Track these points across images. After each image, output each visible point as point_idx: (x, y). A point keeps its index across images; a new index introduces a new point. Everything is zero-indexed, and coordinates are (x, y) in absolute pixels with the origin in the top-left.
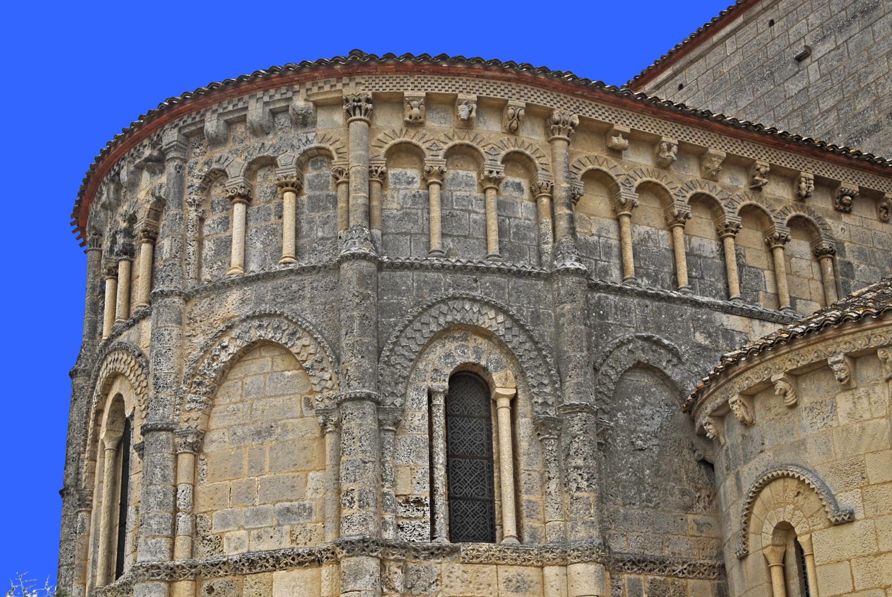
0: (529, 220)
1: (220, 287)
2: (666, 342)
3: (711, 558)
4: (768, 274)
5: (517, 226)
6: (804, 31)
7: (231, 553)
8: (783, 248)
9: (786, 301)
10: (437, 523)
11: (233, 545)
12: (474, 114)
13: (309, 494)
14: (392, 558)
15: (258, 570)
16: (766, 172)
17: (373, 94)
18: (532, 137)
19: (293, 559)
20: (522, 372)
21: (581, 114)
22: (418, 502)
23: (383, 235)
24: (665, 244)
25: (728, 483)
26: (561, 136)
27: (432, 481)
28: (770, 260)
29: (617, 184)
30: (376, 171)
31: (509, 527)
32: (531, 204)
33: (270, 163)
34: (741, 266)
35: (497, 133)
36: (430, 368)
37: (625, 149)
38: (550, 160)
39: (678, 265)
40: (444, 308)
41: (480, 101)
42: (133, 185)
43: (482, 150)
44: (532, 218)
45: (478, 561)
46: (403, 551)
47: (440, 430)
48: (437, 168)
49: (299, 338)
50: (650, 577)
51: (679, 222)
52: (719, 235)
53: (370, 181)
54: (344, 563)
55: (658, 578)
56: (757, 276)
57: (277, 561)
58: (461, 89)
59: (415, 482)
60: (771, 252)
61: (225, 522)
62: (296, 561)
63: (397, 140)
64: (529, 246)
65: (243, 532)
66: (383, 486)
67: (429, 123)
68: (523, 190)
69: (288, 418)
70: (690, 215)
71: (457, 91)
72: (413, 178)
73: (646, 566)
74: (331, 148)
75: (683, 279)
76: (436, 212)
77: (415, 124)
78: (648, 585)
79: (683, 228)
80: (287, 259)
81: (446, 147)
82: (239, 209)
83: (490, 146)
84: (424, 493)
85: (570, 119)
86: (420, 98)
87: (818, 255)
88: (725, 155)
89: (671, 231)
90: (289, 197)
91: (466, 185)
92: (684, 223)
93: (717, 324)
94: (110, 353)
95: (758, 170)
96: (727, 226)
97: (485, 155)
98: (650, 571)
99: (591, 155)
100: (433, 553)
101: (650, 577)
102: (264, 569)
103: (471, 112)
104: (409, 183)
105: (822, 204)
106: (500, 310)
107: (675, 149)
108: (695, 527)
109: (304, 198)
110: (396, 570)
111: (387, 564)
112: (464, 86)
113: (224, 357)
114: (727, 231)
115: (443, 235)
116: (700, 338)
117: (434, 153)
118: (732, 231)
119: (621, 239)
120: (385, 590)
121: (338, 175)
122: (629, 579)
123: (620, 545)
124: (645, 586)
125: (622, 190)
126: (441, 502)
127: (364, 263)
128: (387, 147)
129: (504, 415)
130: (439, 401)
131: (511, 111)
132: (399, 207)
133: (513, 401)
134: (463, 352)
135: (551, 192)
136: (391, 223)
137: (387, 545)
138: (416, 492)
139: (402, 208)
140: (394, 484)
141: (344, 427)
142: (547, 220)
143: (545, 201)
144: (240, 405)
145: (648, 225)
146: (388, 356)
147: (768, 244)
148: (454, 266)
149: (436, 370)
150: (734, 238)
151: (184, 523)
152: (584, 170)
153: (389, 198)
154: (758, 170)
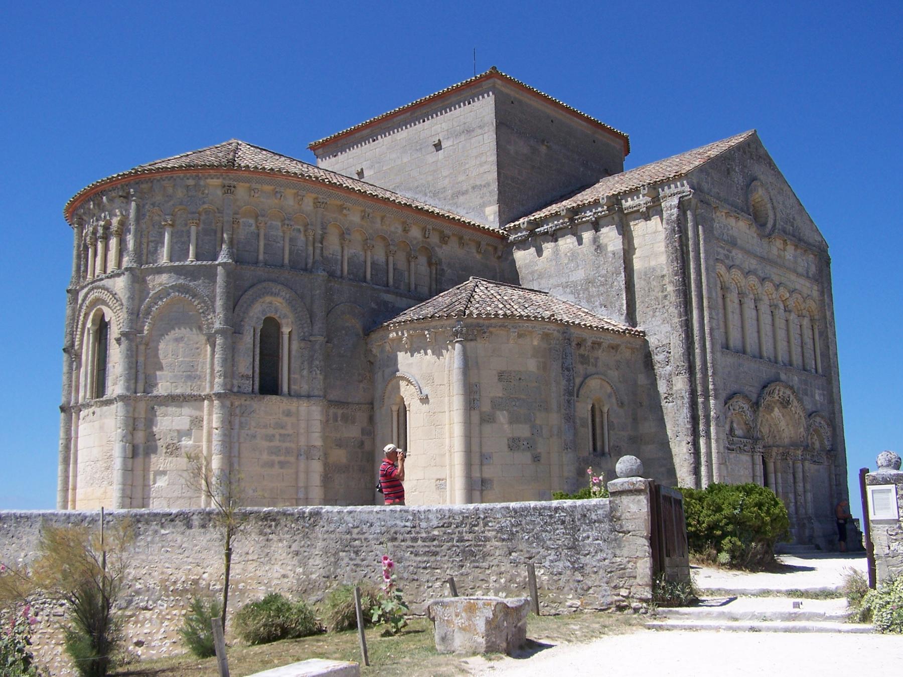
6: (439, 130)
9: (413, 287)
27: (253, 367)
31: (285, 388)
76: (262, 243)
84: (250, 373)
87: (430, 264)
94: (98, 287)
109: (200, 228)
115: (264, 253)
116: (373, 305)
119: (342, 256)
142: (311, 249)
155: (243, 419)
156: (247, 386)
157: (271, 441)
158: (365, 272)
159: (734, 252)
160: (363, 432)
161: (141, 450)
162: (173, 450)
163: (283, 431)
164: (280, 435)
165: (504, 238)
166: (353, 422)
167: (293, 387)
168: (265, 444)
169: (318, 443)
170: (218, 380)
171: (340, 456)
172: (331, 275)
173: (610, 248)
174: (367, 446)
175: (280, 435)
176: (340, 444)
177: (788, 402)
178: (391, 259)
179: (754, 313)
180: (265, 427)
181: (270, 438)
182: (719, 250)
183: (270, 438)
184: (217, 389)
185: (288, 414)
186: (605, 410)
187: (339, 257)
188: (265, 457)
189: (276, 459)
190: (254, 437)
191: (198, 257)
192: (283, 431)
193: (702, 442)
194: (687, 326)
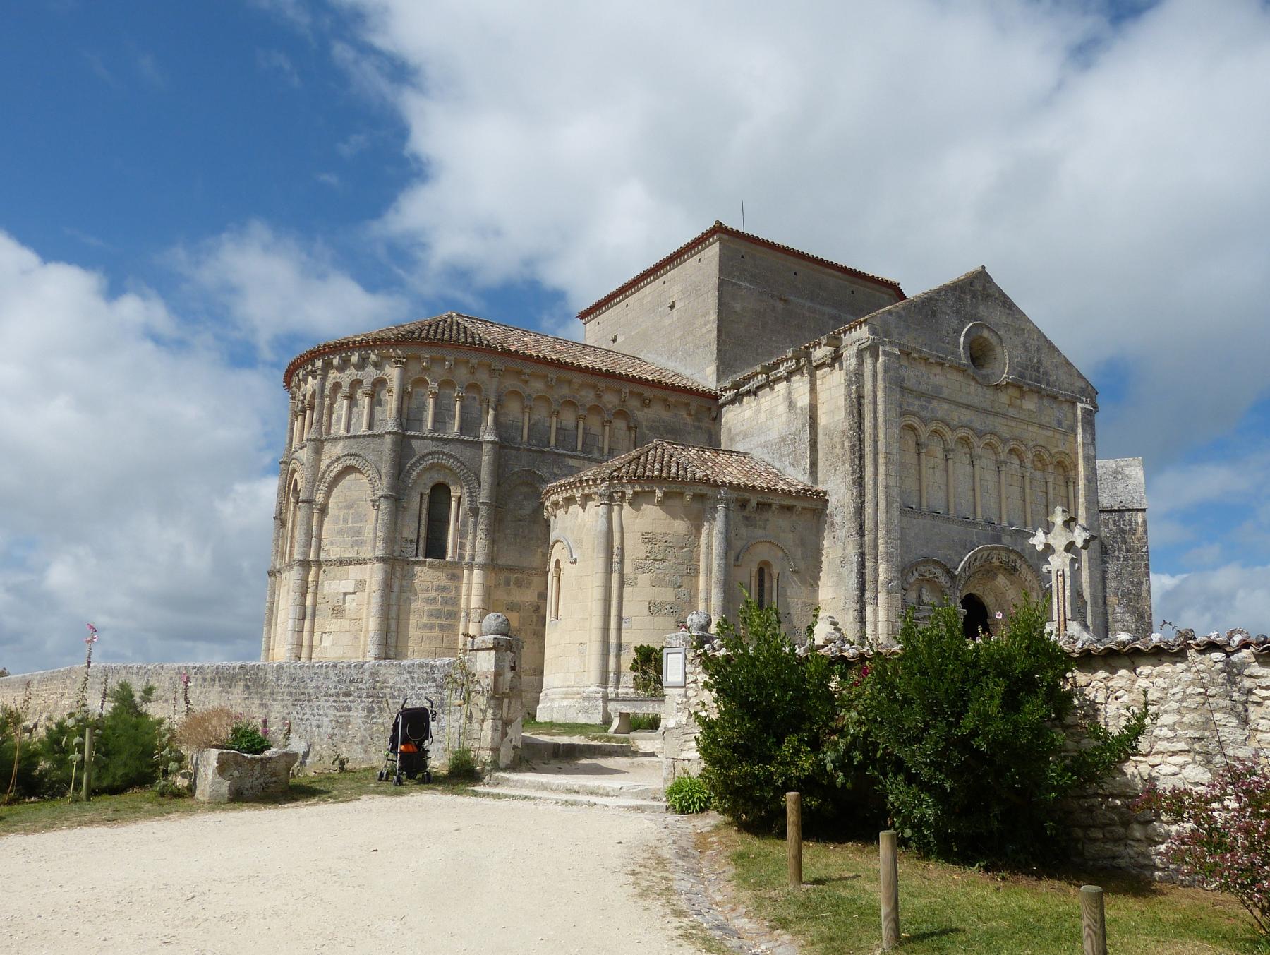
7: (333, 557)
18: (482, 376)
22: (411, 541)
33: (360, 382)
47: (424, 511)
57: (350, 562)
61: (332, 543)
75: (553, 442)
84: (414, 537)
87: (629, 428)
99: (510, 383)
100: (415, 563)
105: (634, 403)
123: (501, 561)
130: (426, 498)
133: (459, 499)
140: (401, 533)
155: (404, 583)
159: (935, 403)
161: (309, 612)
162: (338, 612)
163: (444, 595)
165: (716, 398)
170: (380, 545)
173: (799, 404)
177: (1014, 568)
178: (581, 424)
179: (969, 469)
181: (430, 601)
182: (911, 400)
183: (430, 601)
184: (380, 553)
186: (775, 572)
188: (425, 620)
191: (462, 429)
192: (444, 595)
193: (869, 610)
194: (859, 482)
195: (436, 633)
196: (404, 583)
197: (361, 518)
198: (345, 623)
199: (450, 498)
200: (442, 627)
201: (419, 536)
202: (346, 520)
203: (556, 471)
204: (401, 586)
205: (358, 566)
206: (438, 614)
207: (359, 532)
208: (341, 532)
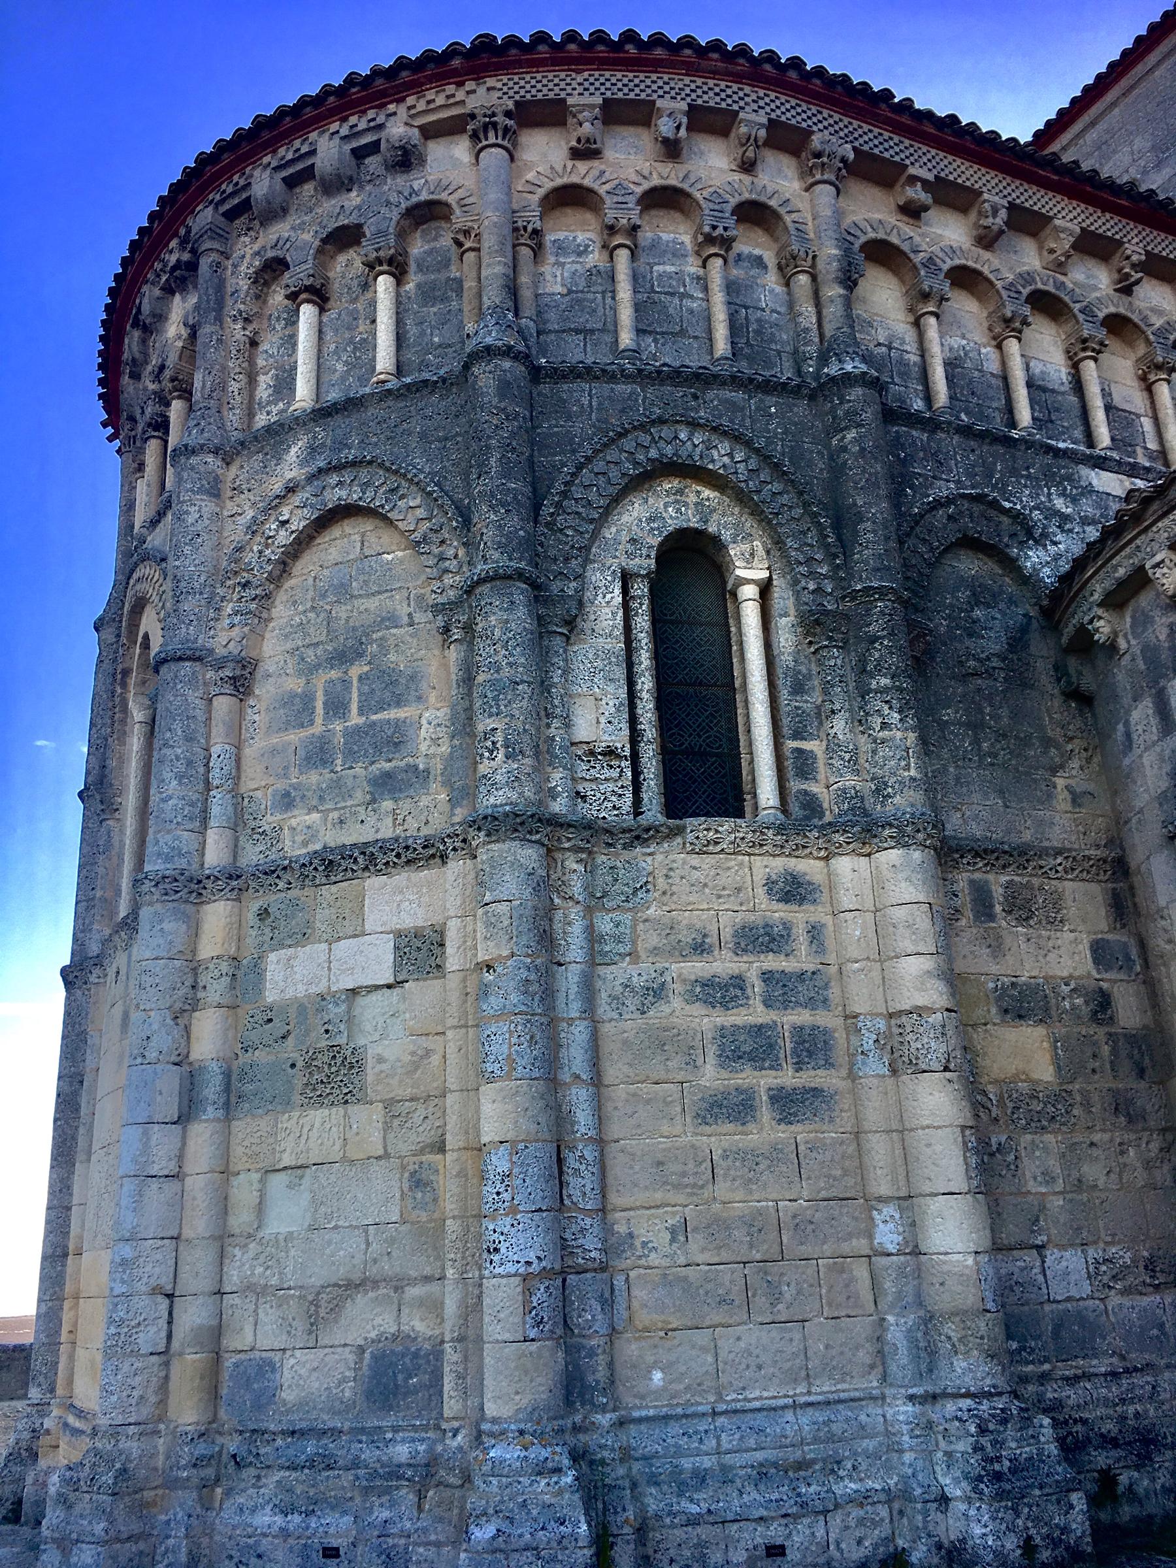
0: (778, 313)
1: (276, 435)
2: (1007, 505)
3: (1098, 846)
4: (1147, 424)
5: (759, 321)
7: (294, 849)
8: (1169, 382)
10: (644, 789)
11: (299, 839)
12: (683, 132)
13: (423, 748)
14: (567, 845)
15: (339, 877)
16: (1141, 262)
17: (517, 103)
18: (780, 180)
19: (398, 856)
20: (779, 542)
21: (856, 144)
22: (610, 752)
23: (539, 333)
24: (993, 366)
25: (1135, 715)
26: (826, 177)
27: (633, 721)
28: (1148, 403)
29: (914, 266)
30: (525, 228)
31: (767, 793)
32: (779, 289)
34: (1109, 408)
35: (721, 170)
36: (624, 537)
37: (926, 208)
38: (810, 218)
39: (1014, 396)
40: (645, 439)
41: (693, 111)
42: (161, 317)
43: (697, 195)
44: (783, 310)
45: (719, 848)
46: (587, 833)
47: (643, 639)
48: (625, 221)
49: (402, 497)
50: (1004, 879)
51: (1013, 330)
52: (1070, 358)
53: (514, 246)
54: (482, 856)
55: (1017, 879)
56: (1130, 424)
58: (661, 92)
59: (603, 720)
60: (1149, 389)
61: (287, 801)
62: (404, 859)
63: (559, 182)
64: (779, 352)
65: (315, 816)
66: (548, 726)
67: (610, 154)
68: (766, 267)
69: (388, 628)
70: (1030, 319)
71: (655, 96)
72: (587, 246)
73: (997, 859)
74: (452, 200)
76: (625, 292)
77: (585, 152)
78: (1001, 891)
79: (1020, 340)
80: (382, 377)
81: (639, 190)
82: (307, 312)
83: (711, 190)
84: (620, 739)
85: (841, 152)
86: (593, 106)
88: (1078, 230)
89: (999, 347)
90: (384, 284)
91: (674, 255)
92: (1020, 332)
93: (1084, 484)
95: (1128, 258)
96: (1084, 341)
97: (702, 202)
98: (1004, 867)
100: (640, 836)
101: (1004, 879)
102: (350, 875)
103: (678, 128)
104: (580, 254)
106: (737, 438)
107: (1003, 214)
108: (1069, 797)
109: (410, 287)
110: (575, 866)
111: (558, 856)
112: (667, 88)
113: (284, 537)
114: (1084, 350)
115: (640, 332)
117: (620, 199)
118: (1093, 350)
120: (557, 901)
121: (461, 238)
122: (972, 882)
124: (998, 892)
125: (923, 273)
126: (649, 754)
127: (507, 364)
128: (541, 192)
129: (750, 615)
130: (640, 589)
131: (743, 129)
132: (565, 291)
133: (765, 589)
134: (678, 511)
135: (813, 266)
136: (552, 315)
137: (554, 822)
138: (606, 737)
139: (570, 292)
140: (568, 724)
141: (479, 628)
143: (803, 279)
144: (312, 615)
145: (963, 337)
146: (552, 514)
147: (1143, 378)
148: (659, 372)
149: (633, 541)
150: (1096, 360)
151: (219, 806)
152: (863, 239)
153: (548, 277)
154: (1128, 258)
156: (608, 796)
157: (726, 1004)
158: (1010, 408)
160: (1100, 952)
161: (212, 1089)
163: (772, 962)
164: (767, 977)
166: (1056, 923)
167: (795, 785)
168: (708, 1021)
169: (934, 995)
171: (1026, 1054)
172: (892, 415)
174: (1129, 1011)
175: (767, 977)
176: (1021, 1004)
180: (700, 948)
181: (722, 992)
185: (793, 890)
187: (914, 358)
188: (711, 1076)
189: (763, 1081)
190: (656, 992)
195: (765, 1131)
196: (604, 924)
197: (393, 687)
198: (367, 1120)
199: (726, 594)
200: (788, 1104)
201: (635, 736)
202: (336, 707)
203: (1059, 503)
204: (593, 937)
205: (401, 877)
206: (755, 1048)
207: (395, 739)
208: (318, 754)
